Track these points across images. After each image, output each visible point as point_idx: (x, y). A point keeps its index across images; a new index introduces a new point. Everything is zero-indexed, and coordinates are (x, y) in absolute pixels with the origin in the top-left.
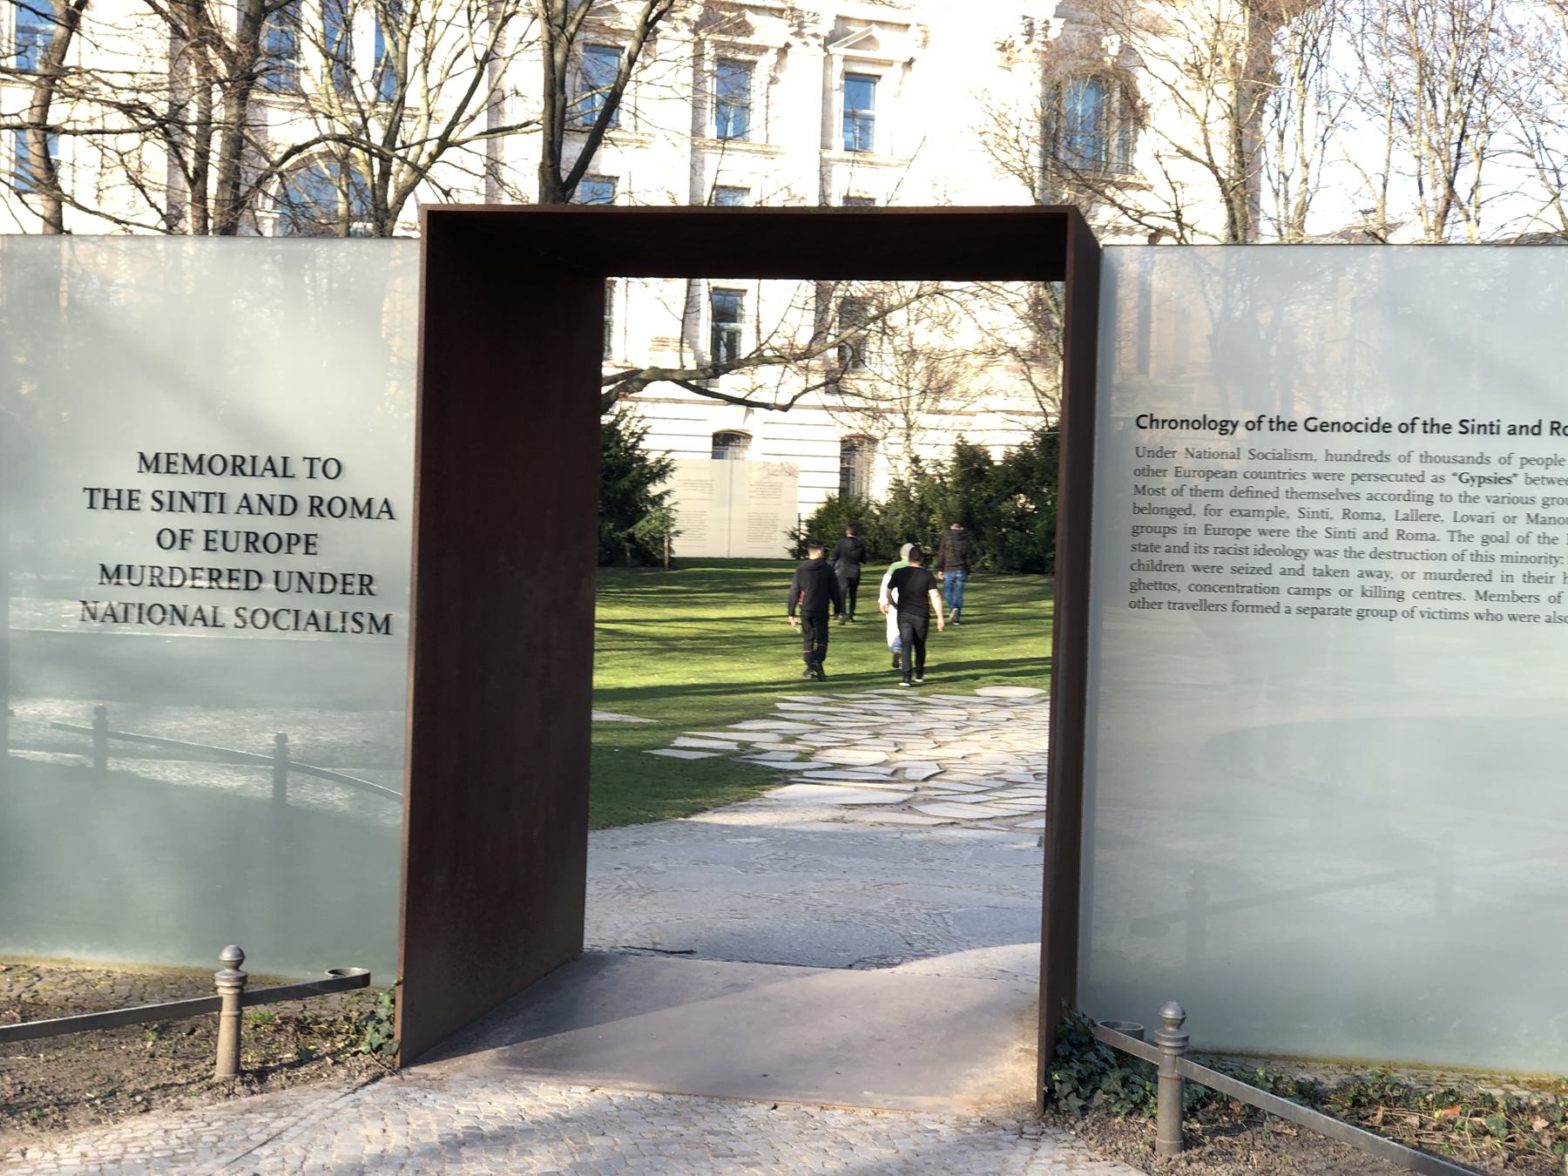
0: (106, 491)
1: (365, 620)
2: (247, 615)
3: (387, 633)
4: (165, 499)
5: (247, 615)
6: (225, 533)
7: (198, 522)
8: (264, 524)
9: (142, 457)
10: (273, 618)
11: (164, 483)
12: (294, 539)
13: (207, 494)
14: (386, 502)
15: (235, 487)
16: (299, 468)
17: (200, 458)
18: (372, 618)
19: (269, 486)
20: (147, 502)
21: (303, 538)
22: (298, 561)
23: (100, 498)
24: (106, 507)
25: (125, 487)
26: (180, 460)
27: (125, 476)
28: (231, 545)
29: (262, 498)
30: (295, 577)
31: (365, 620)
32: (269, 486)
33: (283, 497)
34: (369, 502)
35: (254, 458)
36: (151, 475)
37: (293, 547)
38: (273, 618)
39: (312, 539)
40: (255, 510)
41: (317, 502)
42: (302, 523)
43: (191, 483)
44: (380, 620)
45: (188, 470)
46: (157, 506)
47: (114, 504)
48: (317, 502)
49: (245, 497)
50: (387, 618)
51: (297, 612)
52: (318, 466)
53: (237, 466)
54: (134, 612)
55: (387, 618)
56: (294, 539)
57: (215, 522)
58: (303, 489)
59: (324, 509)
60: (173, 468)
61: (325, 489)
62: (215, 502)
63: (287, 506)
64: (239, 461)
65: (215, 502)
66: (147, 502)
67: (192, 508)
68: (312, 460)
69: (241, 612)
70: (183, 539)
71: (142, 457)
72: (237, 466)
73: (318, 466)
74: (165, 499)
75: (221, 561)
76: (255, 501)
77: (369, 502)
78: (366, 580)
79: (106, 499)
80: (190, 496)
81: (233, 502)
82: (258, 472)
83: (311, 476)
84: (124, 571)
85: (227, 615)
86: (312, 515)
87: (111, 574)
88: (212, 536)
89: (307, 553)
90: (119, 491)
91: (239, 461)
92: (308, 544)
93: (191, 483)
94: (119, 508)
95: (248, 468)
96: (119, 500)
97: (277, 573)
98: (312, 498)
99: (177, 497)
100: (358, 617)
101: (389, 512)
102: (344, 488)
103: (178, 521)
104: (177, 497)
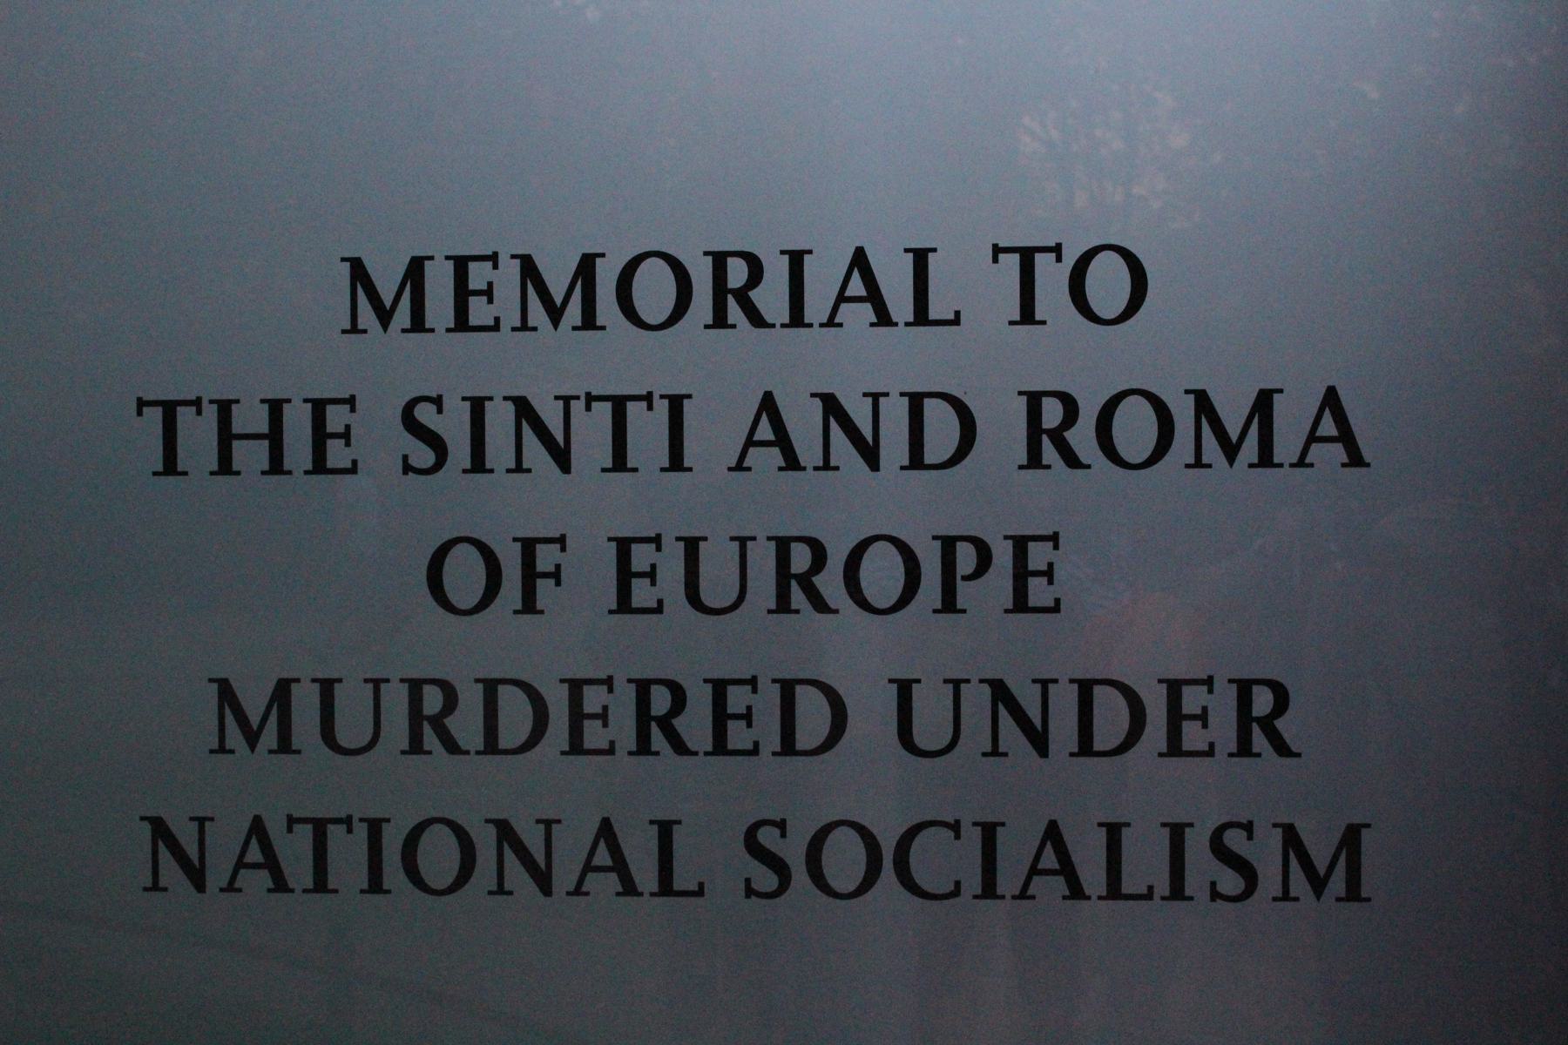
0: (225, 408)
1: (1266, 853)
2: (793, 852)
3: (1353, 892)
4: (453, 426)
5: (793, 852)
6: (692, 546)
9: (359, 272)
12: (966, 558)
13: (619, 404)
14: (1331, 399)
17: (586, 267)
18: (1291, 839)
21: (1003, 555)
23: (197, 434)
24: (225, 466)
25: (297, 389)
29: (831, 406)
30: (977, 699)
31: (1266, 853)
34: (1264, 403)
35: (797, 259)
36: (396, 340)
37: (965, 593)
39: (1038, 556)
40: (809, 452)
41: (1052, 413)
45: (537, 313)
46: (423, 456)
47: (250, 456)
48: (1052, 413)
49: (768, 404)
50: (1352, 838)
51: (989, 831)
52: (1052, 278)
54: (347, 852)
56: (966, 558)
59: (1082, 437)
60: (479, 312)
62: (647, 428)
64: (737, 274)
65: (647, 428)
67: (562, 457)
68: (1027, 256)
69: (767, 837)
70: (530, 575)
71: (359, 272)
73: (1052, 278)
74: (453, 426)
76: (804, 424)
77: (1264, 403)
78: (1263, 702)
79: (226, 436)
80: (552, 416)
82: (817, 308)
83: (1028, 315)
84: (305, 702)
86: (1034, 460)
88: (641, 557)
89: (1021, 604)
90: (276, 408)
91: (737, 274)
92: (1021, 574)
94: (276, 466)
95: (772, 297)
97: (905, 688)
98: (1034, 400)
99: (500, 419)
100: (1234, 839)
101: (1346, 436)
104: (500, 419)
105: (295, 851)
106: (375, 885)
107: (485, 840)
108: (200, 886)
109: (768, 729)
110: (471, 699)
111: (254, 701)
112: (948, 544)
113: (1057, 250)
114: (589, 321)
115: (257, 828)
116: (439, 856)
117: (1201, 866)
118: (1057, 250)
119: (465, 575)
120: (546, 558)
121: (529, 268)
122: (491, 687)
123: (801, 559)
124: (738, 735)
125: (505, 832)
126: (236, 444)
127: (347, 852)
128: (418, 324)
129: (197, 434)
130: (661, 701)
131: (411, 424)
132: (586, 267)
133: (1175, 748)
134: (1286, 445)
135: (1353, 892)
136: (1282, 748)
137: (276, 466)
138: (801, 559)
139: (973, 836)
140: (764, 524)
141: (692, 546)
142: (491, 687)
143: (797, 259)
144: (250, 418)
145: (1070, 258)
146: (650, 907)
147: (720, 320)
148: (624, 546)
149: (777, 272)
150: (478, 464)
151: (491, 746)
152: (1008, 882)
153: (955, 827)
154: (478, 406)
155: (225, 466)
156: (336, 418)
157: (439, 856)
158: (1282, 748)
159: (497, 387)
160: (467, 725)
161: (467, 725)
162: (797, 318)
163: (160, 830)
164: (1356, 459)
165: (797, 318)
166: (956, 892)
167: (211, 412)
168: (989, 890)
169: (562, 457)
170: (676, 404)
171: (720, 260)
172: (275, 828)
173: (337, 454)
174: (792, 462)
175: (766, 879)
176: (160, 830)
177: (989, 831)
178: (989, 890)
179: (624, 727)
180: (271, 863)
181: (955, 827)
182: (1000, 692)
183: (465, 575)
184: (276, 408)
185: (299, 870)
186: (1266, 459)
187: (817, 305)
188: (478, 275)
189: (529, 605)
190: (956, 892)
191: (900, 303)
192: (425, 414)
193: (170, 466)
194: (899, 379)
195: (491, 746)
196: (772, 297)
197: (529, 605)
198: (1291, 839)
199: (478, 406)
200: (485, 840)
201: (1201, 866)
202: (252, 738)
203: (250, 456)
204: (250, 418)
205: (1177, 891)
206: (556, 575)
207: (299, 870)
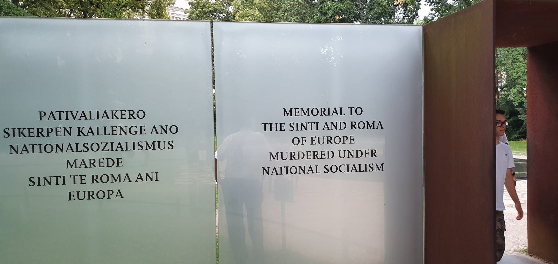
0: (271, 124)
2: (329, 168)
3: (382, 170)
5: (329, 168)
6: (319, 137)
7: (308, 134)
8: (334, 133)
10: (338, 169)
11: (294, 119)
14: (380, 122)
15: (321, 120)
16: (346, 111)
17: (308, 109)
18: (377, 165)
19: (336, 119)
20: (287, 127)
21: (349, 138)
22: (347, 146)
23: (268, 127)
26: (300, 110)
27: (279, 118)
28: (321, 142)
30: (347, 152)
32: (336, 119)
33: (341, 123)
35: (329, 109)
38: (338, 169)
40: (330, 128)
41: (354, 124)
42: (348, 132)
43: (304, 119)
44: (379, 166)
45: (303, 114)
46: (292, 129)
47: (274, 129)
48: (354, 124)
50: (382, 165)
51: (348, 165)
52: (353, 110)
53: (323, 113)
54: (284, 170)
55: (382, 165)
57: (315, 133)
58: (348, 119)
59: (356, 126)
60: (297, 114)
61: (356, 118)
62: (314, 126)
63: (342, 126)
64: (323, 110)
65: (314, 126)
66: (287, 127)
67: (306, 129)
68: (351, 108)
69: (326, 167)
70: (303, 141)
72: (322, 112)
73: (353, 110)
75: (318, 148)
76: (330, 125)
79: (271, 127)
81: (321, 126)
82: (331, 114)
83: (351, 114)
84: (280, 155)
85: (321, 169)
86: (352, 129)
87: (274, 157)
90: (276, 124)
91: (323, 110)
92: (351, 140)
93: (304, 119)
94: (276, 130)
95: (326, 112)
96: (276, 127)
99: (299, 125)
101: (381, 126)
102: (364, 118)
103: (300, 134)
104: (299, 125)
105: (279, 171)
106: (287, 174)
107: (298, 168)
108: (269, 175)
109: (326, 156)
110: (297, 154)
111: (274, 155)
112: (344, 137)
113: (354, 108)
114: (308, 115)
115: (275, 168)
116: (293, 170)
117: (368, 168)
118: (354, 108)
119: (296, 141)
120: (304, 139)
121: (302, 110)
122: (299, 152)
123: (329, 139)
124: (323, 156)
125: (300, 167)
126: (272, 128)
127: (284, 170)
128: (291, 115)
129: (268, 127)
130: (316, 153)
131: (290, 126)
132: (308, 109)
133: (365, 157)
134: (376, 127)
135: (382, 170)
136: (376, 156)
137: (276, 130)
138: (329, 139)
139: (346, 166)
140: (326, 136)
141: (319, 137)
142: (299, 152)
143: (329, 109)
144: (274, 125)
145: (355, 108)
146: (315, 174)
147: (321, 115)
148: (312, 138)
149: (327, 110)
150: (297, 130)
151: (299, 159)
152: (350, 170)
153: (345, 165)
154: (297, 124)
155: (271, 130)
156: (283, 125)
157: (293, 170)
158: (376, 156)
159: (299, 122)
160: (296, 156)
161: (296, 156)
162: (329, 115)
163: (264, 169)
164: (382, 128)
165: (329, 115)
166: (345, 172)
167: (270, 124)
168: (348, 171)
169: (306, 129)
170: (317, 123)
171: (321, 109)
172: (276, 168)
173: (283, 129)
174: (329, 129)
175: (326, 171)
176: (264, 169)
177: (348, 165)
178: (348, 171)
179: (312, 156)
180: (276, 172)
181: (345, 165)
182: (349, 151)
183: (296, 141)
184: (276, 124)
185: (279, 172)
186: (374, 128)
187: (331, 113)
188: (297, 110)
189: (303, 144)
190: (345, 172)
191: (339, 113)
192: (292, 124)
193: (265, 130)
194: (339, 121)
195: (299, 159)
196: (326, 112)
197: (303, 144)
198: (377, 165)
199: (297, 124)
200: (298, 168)
201: (368, 168)
202: (274, 159)
203: (274, 129)
204: (274, 125)
205: (366, 171)
206: (305, 141)
207: (279, 172)
